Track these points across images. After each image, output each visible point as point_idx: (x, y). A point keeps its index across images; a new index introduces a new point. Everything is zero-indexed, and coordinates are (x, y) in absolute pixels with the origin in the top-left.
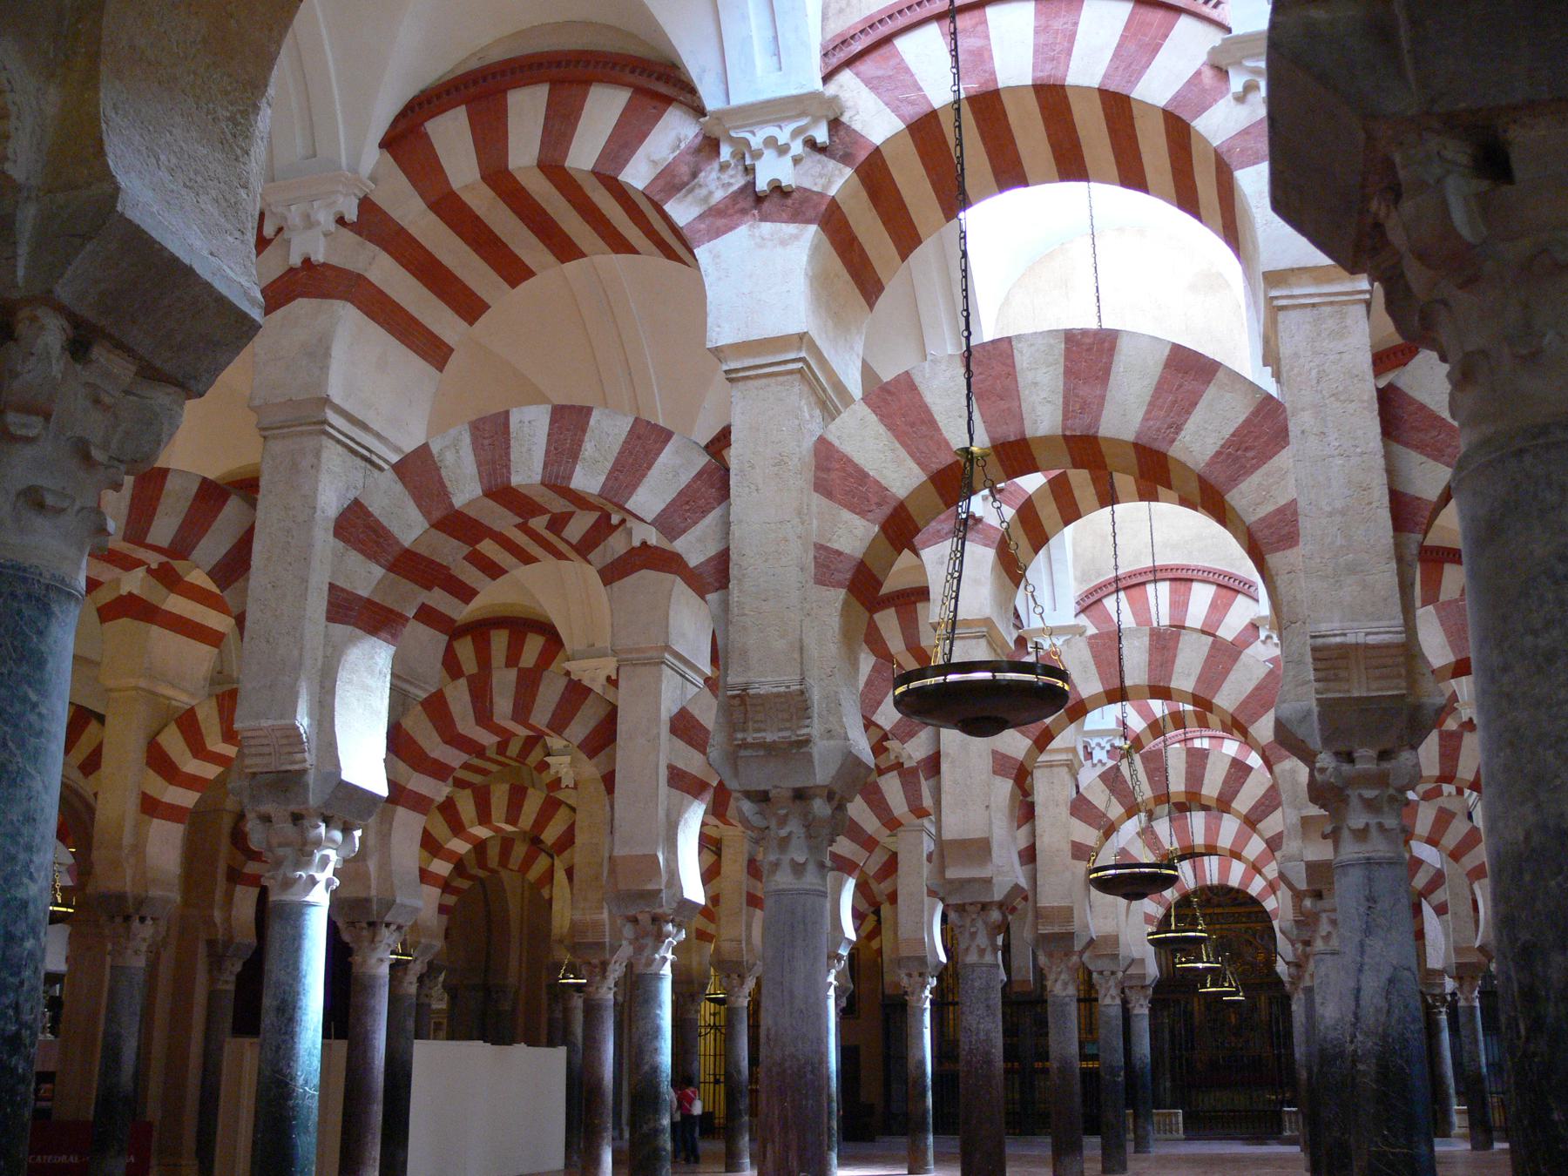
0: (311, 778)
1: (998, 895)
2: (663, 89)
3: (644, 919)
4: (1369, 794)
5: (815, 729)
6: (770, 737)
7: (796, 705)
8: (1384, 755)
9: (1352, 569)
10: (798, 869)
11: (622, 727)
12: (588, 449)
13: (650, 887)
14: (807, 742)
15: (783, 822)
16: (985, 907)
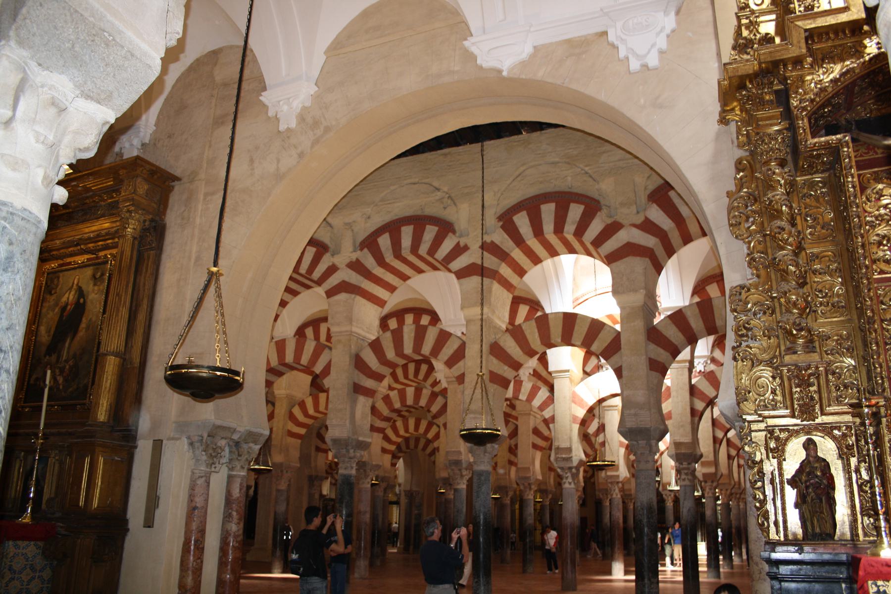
0: (463, 461)
1: (621, 479)
2: (537, 307)
3: (526, 484)
4: (686, 471)
5: (573, 454)
6: (564, 456)
7: (569, 450)
8: (689, 464)
9: (682, 426)
10: (570, 483)
11: (520, 432)
12: (523, 390)
13: (528, 475)
14: (571, 457)
15: (566, 473)
16: (618, 483)
